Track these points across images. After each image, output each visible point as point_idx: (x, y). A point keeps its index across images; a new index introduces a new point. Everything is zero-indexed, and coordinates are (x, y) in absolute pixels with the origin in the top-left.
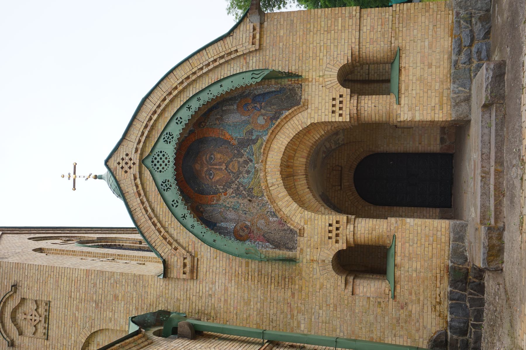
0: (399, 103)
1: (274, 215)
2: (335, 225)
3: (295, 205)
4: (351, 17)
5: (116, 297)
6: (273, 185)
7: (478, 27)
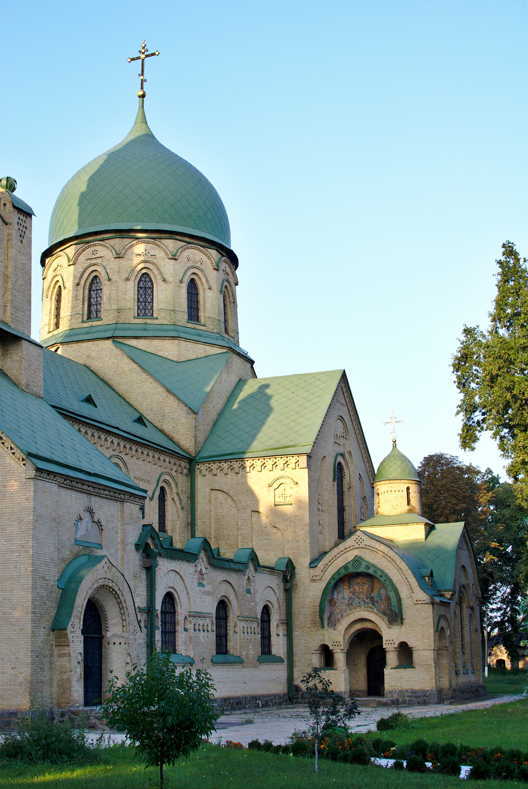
0: (392, 668)
1: (342, 616)
2: (339, 644)
3: (346, 626)
4: (429, 646)
5: (298, 541)
6: (354, 615)
7: (421, 699)
